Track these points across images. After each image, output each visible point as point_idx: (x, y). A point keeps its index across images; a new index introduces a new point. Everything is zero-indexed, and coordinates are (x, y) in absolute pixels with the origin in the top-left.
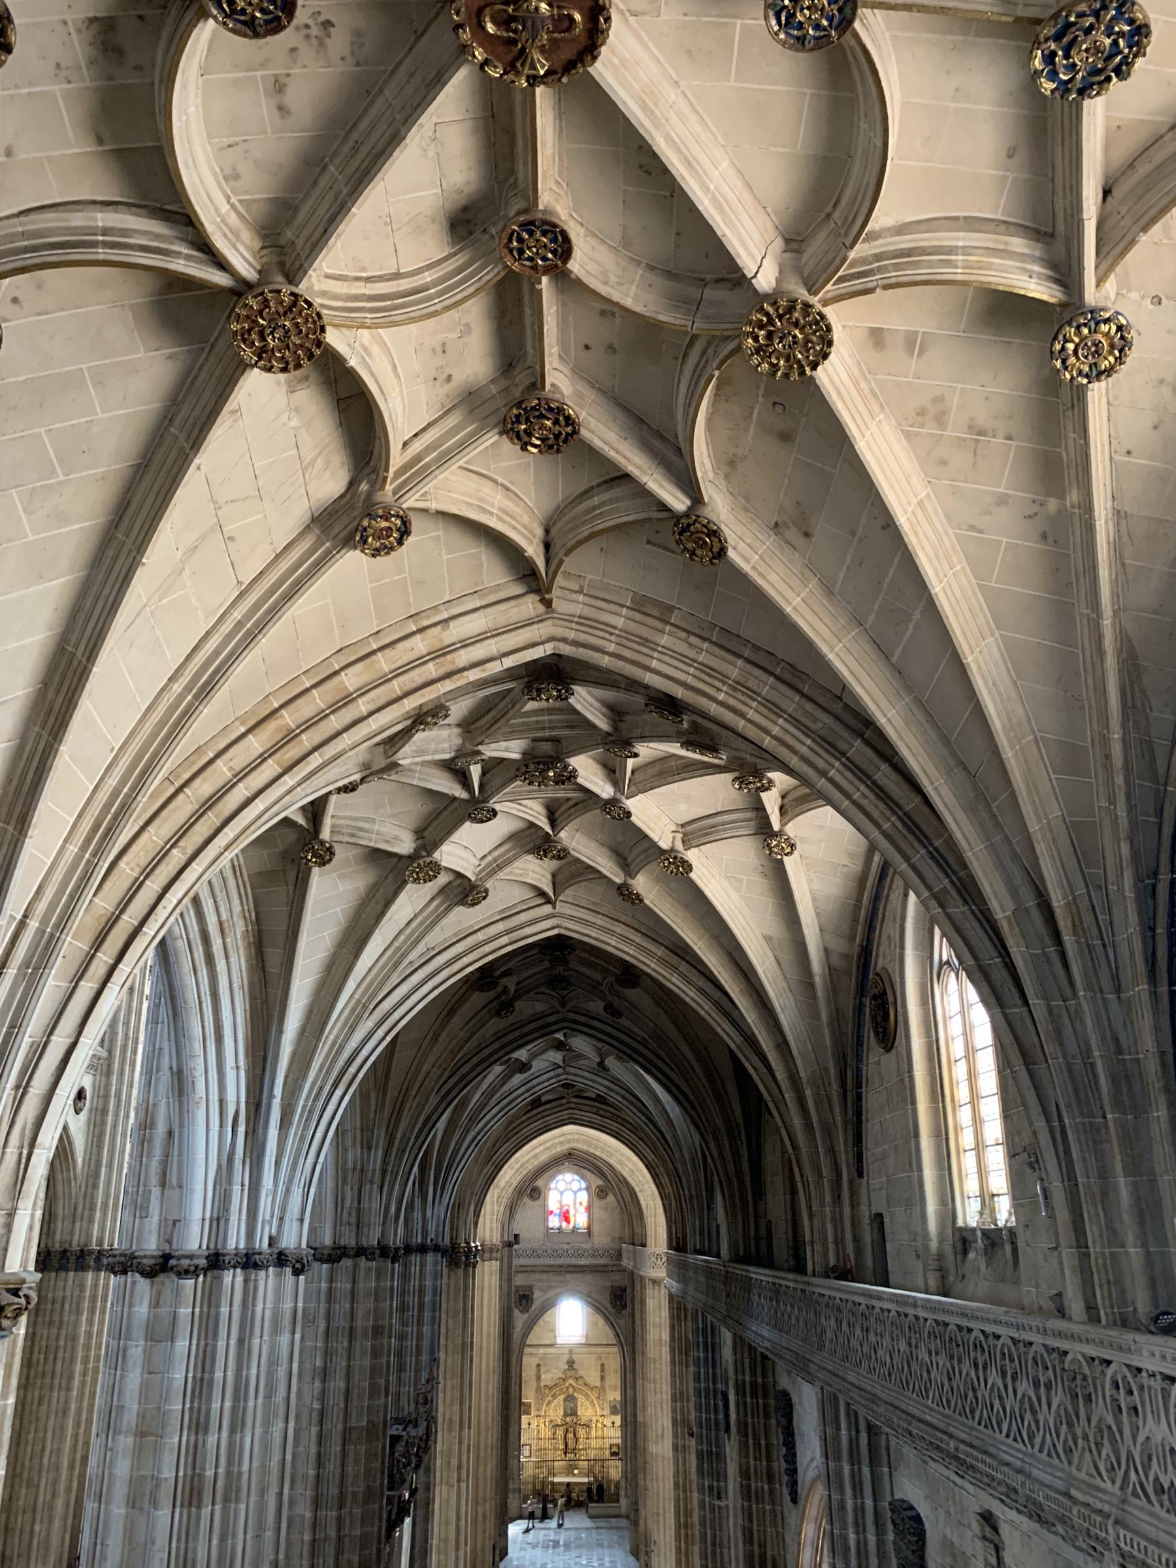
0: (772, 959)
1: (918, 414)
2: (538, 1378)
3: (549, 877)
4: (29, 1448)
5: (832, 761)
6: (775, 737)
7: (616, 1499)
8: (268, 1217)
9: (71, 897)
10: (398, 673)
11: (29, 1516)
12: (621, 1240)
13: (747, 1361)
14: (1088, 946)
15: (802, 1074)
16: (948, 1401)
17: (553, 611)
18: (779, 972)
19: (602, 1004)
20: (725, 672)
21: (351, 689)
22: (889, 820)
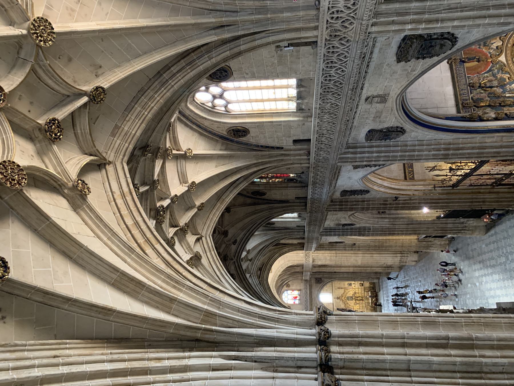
3: (193, 236)
6: (160, 99)
7: (374, 284)
12: (302, 280)
13: (333, 207)
15: (255, 162)
17: (113, 162)
19: (233, 245)
21: (133, 222)
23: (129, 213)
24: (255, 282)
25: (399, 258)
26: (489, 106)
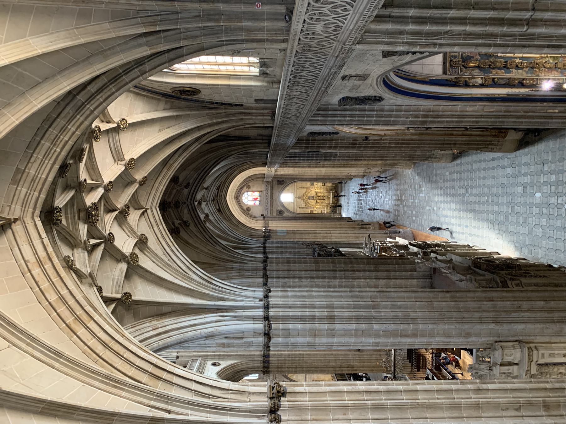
2: (303, 208)
3: (136, 211)
4: (319, 364)
6: (76, 130)
8: (253, 302)
9: (142, 391)
10: (49, 279)
11: (337, 361)
12: (263, 181)
13: (299, 145)
14: (160, 21)
15: (209, 122)
16: (311, 88)
18: (172, 128)
19: (185, 190)
20: (47, 148)
21: (57, 297)
22: (111, 89)
23: (50, 286)
24: (211, 210)
25: (363, 170)
26: (478, 67)
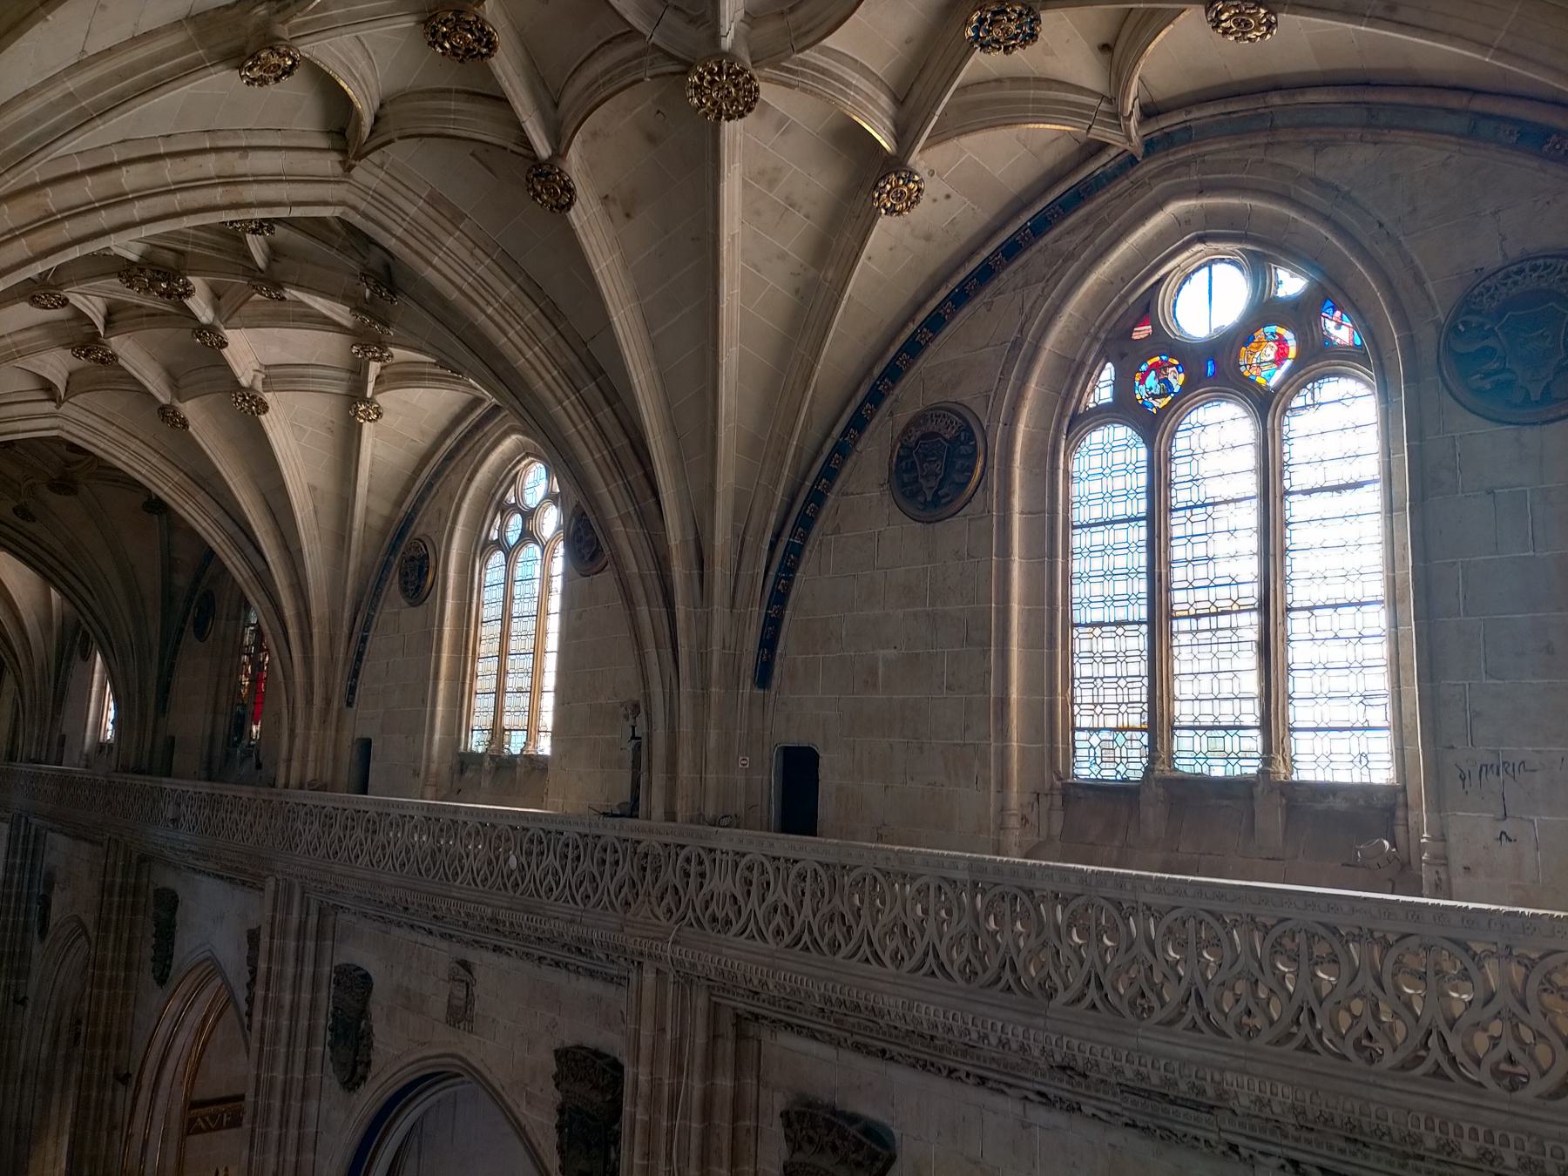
0: (311, 508)
1: (759, 173)
3: (66, 374)
5: (570, 394)
17: (350, 177)
21: (127, 188)
